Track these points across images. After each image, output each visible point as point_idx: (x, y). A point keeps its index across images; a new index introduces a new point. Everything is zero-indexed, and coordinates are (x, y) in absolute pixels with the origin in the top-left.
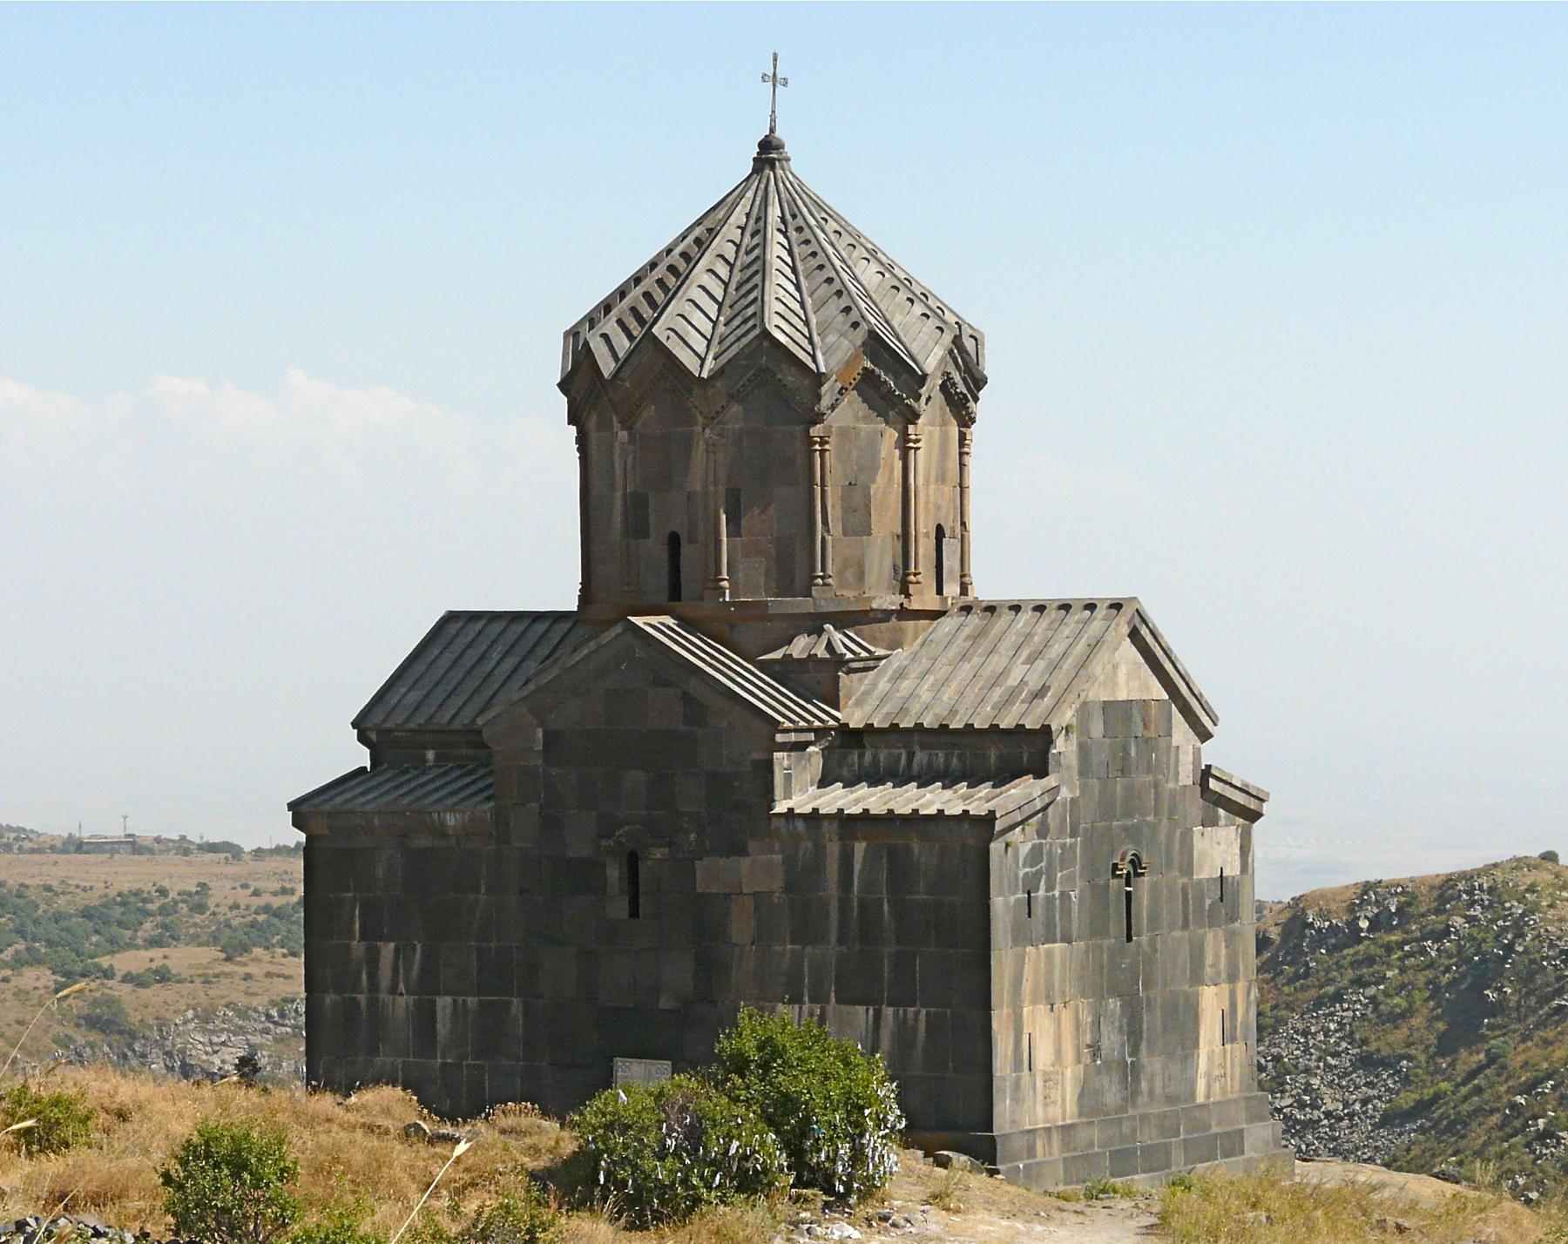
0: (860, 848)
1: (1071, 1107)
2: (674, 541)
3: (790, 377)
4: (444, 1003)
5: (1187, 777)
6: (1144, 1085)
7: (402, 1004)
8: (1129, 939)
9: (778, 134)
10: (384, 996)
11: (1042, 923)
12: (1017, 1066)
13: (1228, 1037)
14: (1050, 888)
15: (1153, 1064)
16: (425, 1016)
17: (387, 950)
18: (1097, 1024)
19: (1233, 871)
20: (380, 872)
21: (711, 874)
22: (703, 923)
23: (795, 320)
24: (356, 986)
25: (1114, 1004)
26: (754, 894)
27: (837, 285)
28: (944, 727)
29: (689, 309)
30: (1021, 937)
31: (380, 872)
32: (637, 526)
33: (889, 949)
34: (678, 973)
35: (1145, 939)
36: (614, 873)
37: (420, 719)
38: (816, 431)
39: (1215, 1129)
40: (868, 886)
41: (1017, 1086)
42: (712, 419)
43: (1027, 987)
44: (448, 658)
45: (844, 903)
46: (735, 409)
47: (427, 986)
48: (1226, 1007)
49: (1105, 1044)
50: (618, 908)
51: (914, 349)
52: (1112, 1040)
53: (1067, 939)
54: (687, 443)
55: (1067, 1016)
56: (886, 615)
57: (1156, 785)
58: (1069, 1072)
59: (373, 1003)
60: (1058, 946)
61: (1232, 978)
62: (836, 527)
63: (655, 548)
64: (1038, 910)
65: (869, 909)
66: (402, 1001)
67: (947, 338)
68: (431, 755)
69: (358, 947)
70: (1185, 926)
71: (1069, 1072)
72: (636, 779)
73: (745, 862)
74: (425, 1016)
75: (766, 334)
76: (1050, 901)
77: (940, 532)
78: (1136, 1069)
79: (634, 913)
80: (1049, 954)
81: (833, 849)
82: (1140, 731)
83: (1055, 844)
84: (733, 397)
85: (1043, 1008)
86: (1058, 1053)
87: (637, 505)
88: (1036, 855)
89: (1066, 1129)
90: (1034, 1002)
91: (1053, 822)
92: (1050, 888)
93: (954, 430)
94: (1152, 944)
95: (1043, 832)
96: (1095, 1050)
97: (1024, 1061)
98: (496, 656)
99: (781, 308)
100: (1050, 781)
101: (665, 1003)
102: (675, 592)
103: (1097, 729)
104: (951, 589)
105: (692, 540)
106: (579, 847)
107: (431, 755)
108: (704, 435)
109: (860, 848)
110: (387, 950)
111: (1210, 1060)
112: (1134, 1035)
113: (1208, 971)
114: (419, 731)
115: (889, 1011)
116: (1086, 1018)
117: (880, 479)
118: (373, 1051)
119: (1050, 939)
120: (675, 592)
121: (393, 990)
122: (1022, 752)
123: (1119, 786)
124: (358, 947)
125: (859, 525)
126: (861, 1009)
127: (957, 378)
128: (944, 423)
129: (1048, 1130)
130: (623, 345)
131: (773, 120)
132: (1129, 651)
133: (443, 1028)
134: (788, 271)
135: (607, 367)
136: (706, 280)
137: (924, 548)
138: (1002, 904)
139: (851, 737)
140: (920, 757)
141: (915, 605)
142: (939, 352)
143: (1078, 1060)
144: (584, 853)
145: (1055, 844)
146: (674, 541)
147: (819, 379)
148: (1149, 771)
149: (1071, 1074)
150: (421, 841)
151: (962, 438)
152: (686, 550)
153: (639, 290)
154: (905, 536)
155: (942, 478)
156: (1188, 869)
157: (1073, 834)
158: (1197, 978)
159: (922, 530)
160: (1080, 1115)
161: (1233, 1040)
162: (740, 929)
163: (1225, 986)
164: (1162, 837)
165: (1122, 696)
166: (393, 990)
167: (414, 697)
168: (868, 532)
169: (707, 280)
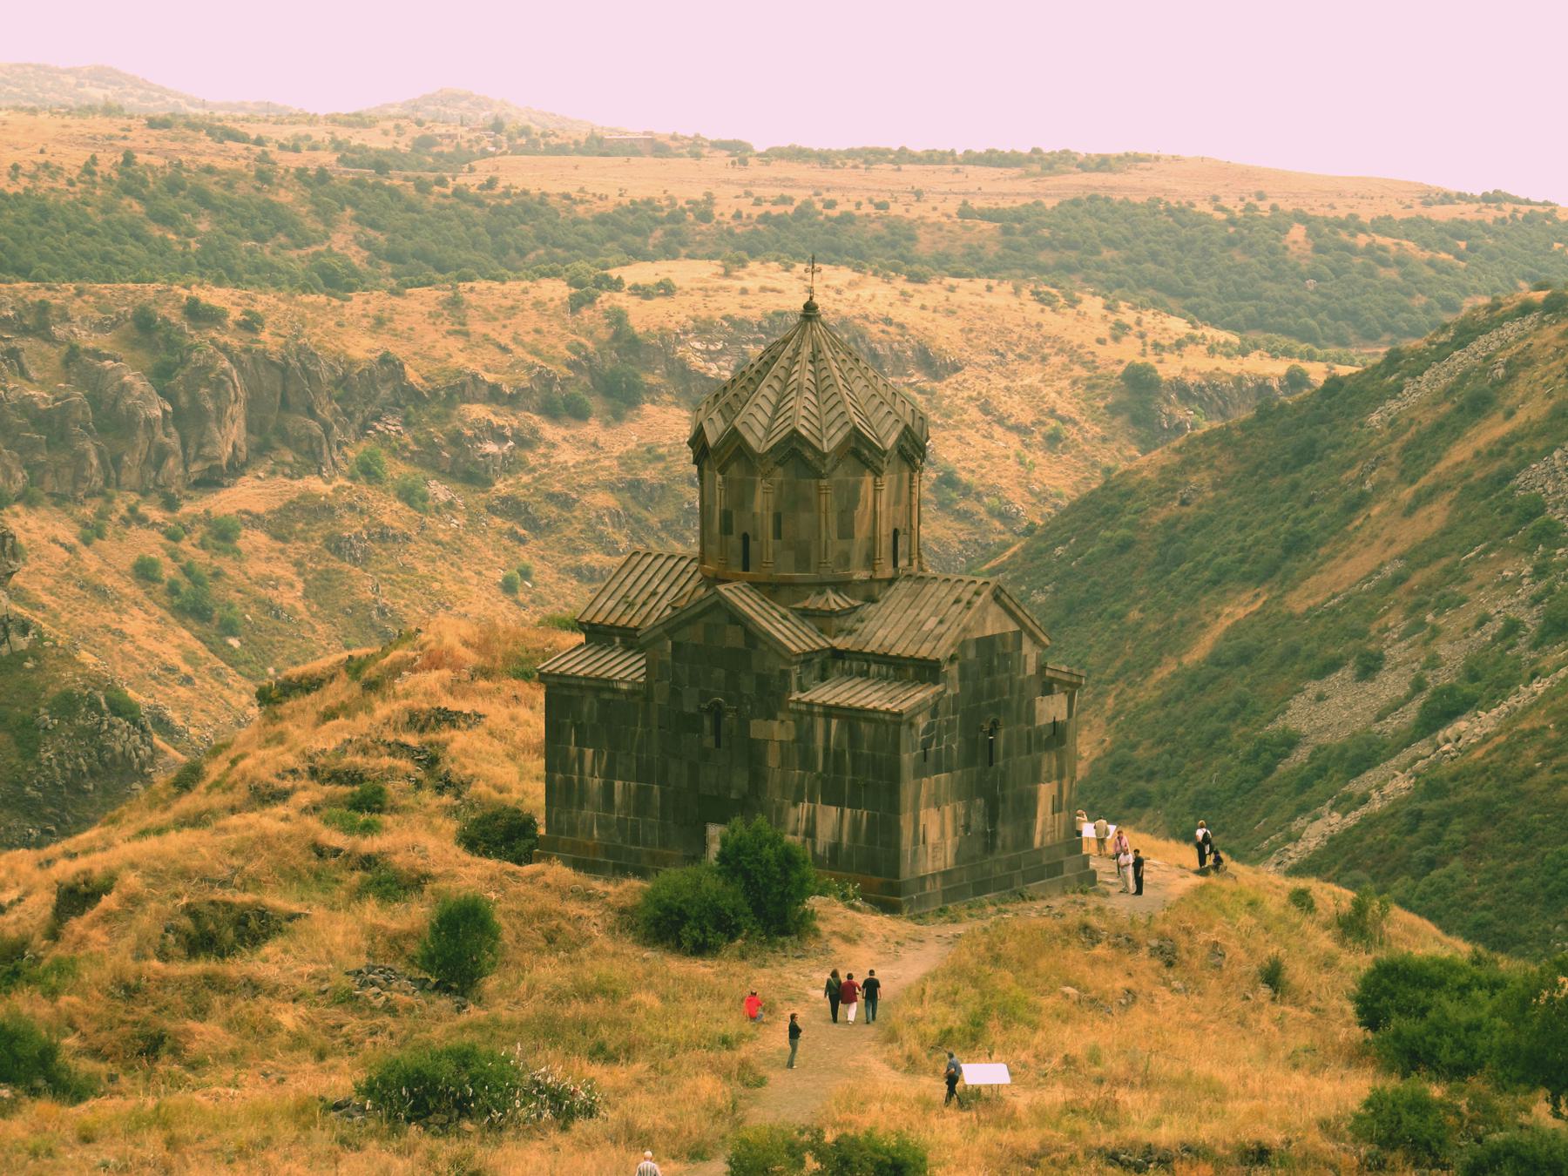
0: (834, 722)
1: (950, 860)
2: (745, 538)
3: (808, 454)
4: (618, 784)
5: (1031, 669)
6: (999, 843)
7: (596, 783)
8: (991, 764)
9: (815, 300)
10: (587, 778)
11: (929, 763)
12: (916, 842)
13: (1057, 808)
14: (939, 744)
15: (1006, 831)
16: (608, 790)
17: (589, 752)
18: (968, 815)
19: (1062, 716)
20: (586, 709)
21: (758, 729)
22: (753, 754)
23: (813, 420)
24: (572, 771)
25: (980, 802)
26: (781, 742)
27: (838, 398)
28: (886, 655)
29: (754, 410)
30: (920, 772)
31: (586, 709)
32: (726, 528)
33: (848, 778)
34: (740, 780)
35: (1001, 763)
36: (707, 723)
37: (611, 620)
38: (824, 483)
39: (1045, 862)
40: (839, 743)
41: (915, 853)
42: (766, 476)
43: (923, 800)
44: (632, 579)
45: (826, 749)
46: (780, 470)
47: (609, 775)
48: (1055, 793)
49: (973, 823)
50: (709, 741)
51: (881, 434)
52: (977, 821)
53: (949, 770)
54: (753, 485)
55: (948, 810)
56: (863, 582)
57: (1011, 678)
58: (949, 842)
59: (581, 781)
60: (943, 776)
61: (1060, 776)
62: (834, 536)
63: (735, 541)
64: (931, 758)
65: (839, 756)
66: (596, 781)
67: (901, 427)
68: (618, 640)
69: (573, 749)
70: (1029, 752)
71: (949, 842)
72: (719, 673)
73: (776, 725)
74: (608, 790)
75: (795, 431)
76: (938, 752)
77: (896, 533)
78: (994, 835)
79: (718, 744)
80: (937, 781)
81: (820, 723)
82: (1001, 650)
83: (942, 720)
84: (779, 463)
85: (933, 810)
86: (943, 833)
87: (726, 517)
88: (928, 730)
89: (946, 875)
90: (927, 807)
91: (941, 708)
92: (939, 744)
93: (906, 475)
94: (1006, 765)
95: (934, 714)
96: (967, 827)
97: (919, 839)
98: (656, 581)
99: (804, 413)
100: (940, 688)
101: (733, 796)
102: (746, 568)
103: (971, 654)
104: (903, 563)
105: (755, 539)
106: (689, 708)
107: (618, 640)
108: (761, 485)
109: (834, 722)
110: (589, 752)
111: (1044, 823)
112: (992, 816)
113: (1044, 775)
114: (612, 626)
115: (848, 811)
116: (961, 811)
117: (861, 508)
118: (581, 806)
119: (938, 771)
120: (746, 568)
121: (592, 775)
122: (926, 671)
123: (986, 682)
124: (573, 749)
125: (846, 533)
126: (833, 809)
127: (908, 447)
128: (901, 471)
129: (933, 875)
130: (720, 425)
131: (811, 290)
132: (994, 609)
133: (618, 798)
134: (812, 388)
135: (711, 439)
136: (767, 392)
137: (885, 544)
138: (907, 758)
139: (837, 654)
140: (874, 668)
141: (879, 576)
142: (894, 436)
143: (956, 834)
144: (693, 710)
145: (942, 720)
146: (745, 538)
147: (824, 456)
148: (1006, 670)
149: (950, 842)
150: (607, 696)
151: (911, 478)
152: (752, 543)
153: (730, 393)
154: (874, 538)
155: (897, 502)
156: (1031, 719)
157: (954, 713)
158: (1036, 778)
159: (884, 532)
160: (957, 863)
161: (1060, 810)
162: (773, 760)
163: (1055, 783)
164: (1014, 705)
165: (989, 632)
166: (592, 775)
167: (611, 604)
168: (852, 536)
169: (766, 391)
